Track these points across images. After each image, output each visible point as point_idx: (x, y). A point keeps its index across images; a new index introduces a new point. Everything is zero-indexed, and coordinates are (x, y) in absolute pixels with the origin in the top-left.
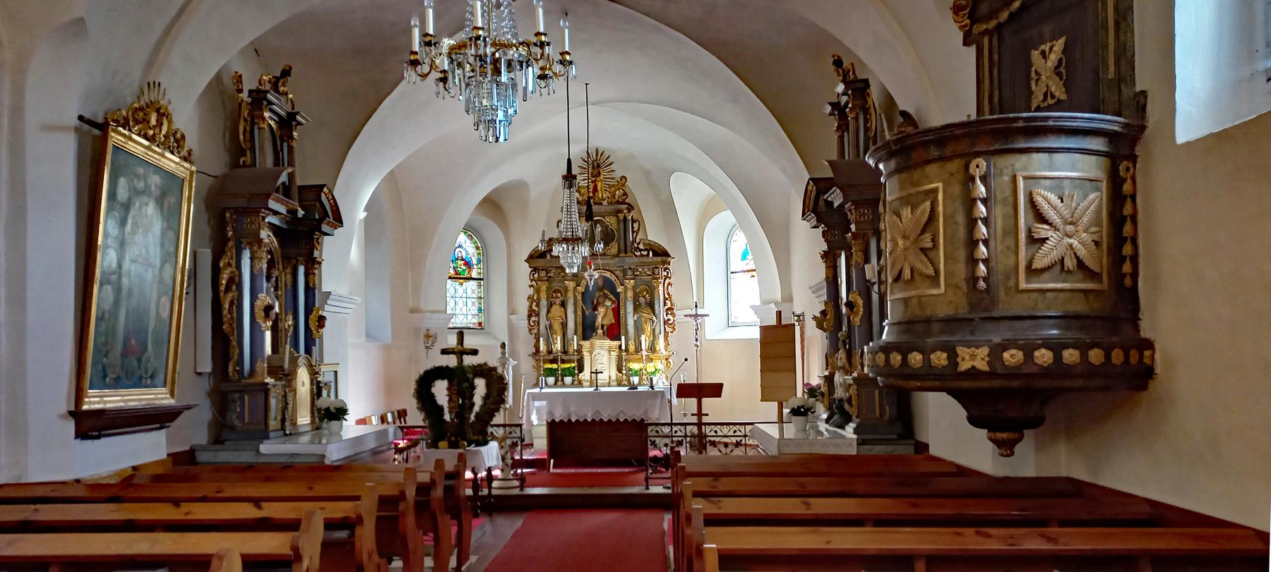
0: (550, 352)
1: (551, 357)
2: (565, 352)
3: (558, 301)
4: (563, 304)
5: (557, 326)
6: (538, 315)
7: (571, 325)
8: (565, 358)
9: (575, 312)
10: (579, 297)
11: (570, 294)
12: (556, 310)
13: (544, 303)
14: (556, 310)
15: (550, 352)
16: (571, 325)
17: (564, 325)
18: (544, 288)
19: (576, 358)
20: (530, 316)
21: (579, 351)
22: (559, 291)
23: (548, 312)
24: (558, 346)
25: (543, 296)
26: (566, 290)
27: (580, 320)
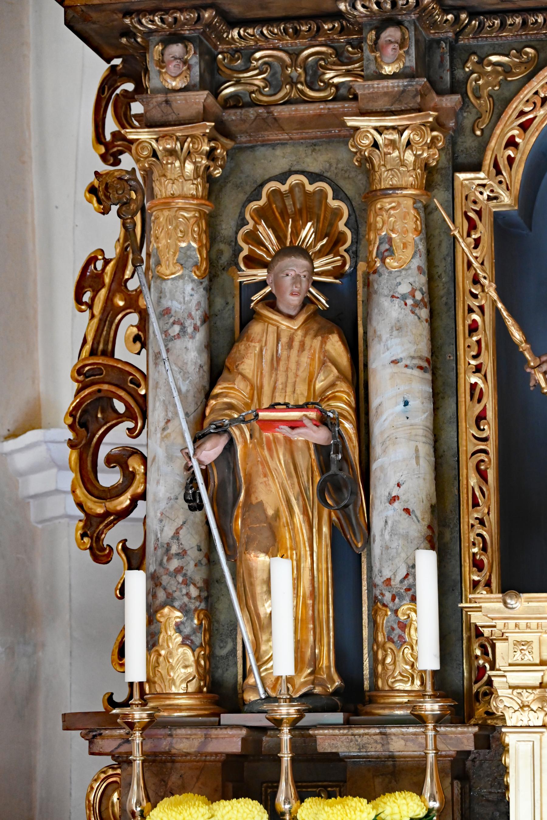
0: (221, 693)
1: (228, 741)
2: (353, 695)
3: (292, 279)
4: (342, 313)
5: (277, 482)
6: (139, 410)
7: (401, 466)
8: (336, 738)
9: (439, 367)
10: (475, 253)
11: (397, 221)
12: (286, 360)
13: (182, 294)
14: (286, 360)
15: (221, 693)
16: (401, 466)
17: (343, 479)
18: (181, 181)
19: (429, 743)
20: (88, 421)
21: (464, 687)
22: (309, 208)
23: (217, 369)
24: (281, 641)
25: (176, 239)
26: (366, 197)
27: (479, 438)
